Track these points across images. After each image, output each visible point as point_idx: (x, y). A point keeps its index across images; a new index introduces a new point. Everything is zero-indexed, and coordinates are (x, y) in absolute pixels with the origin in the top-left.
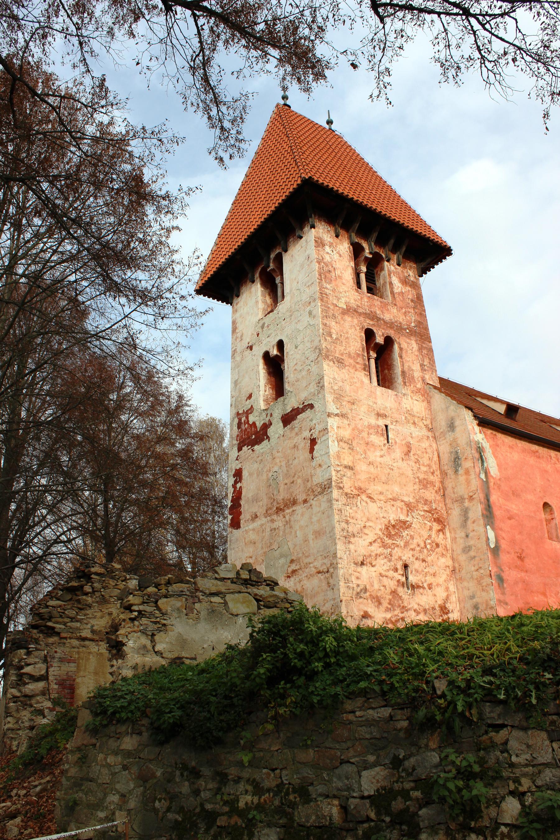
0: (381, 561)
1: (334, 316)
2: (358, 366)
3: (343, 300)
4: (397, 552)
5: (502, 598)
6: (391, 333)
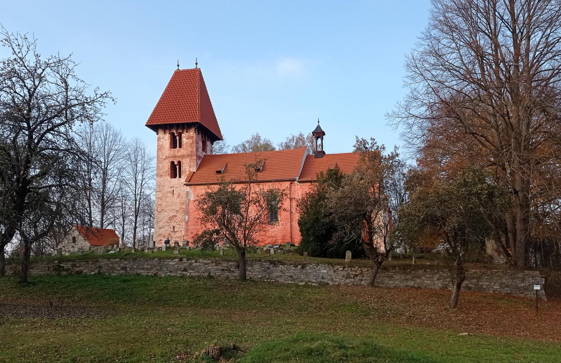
0: (166, 227)
4: (172, 224)
5: (186, 234)
6: (180, 159)
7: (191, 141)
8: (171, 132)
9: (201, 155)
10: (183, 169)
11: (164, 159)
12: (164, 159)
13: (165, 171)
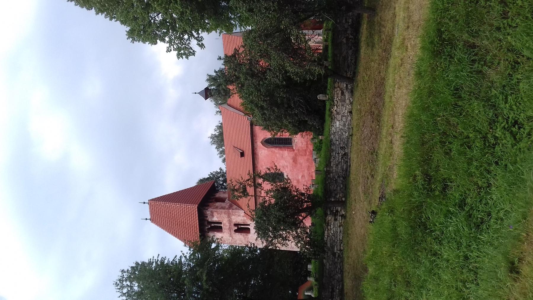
1: (235, 241)
2: (247, 237)
3: (229, 238)
6: (232, 224)
7: (215, 214)
8: (207, 230)
9: (228, 204)
10: (241, 221)
11: (232, 238)
12: (232, 238)
13: (243, 238)
